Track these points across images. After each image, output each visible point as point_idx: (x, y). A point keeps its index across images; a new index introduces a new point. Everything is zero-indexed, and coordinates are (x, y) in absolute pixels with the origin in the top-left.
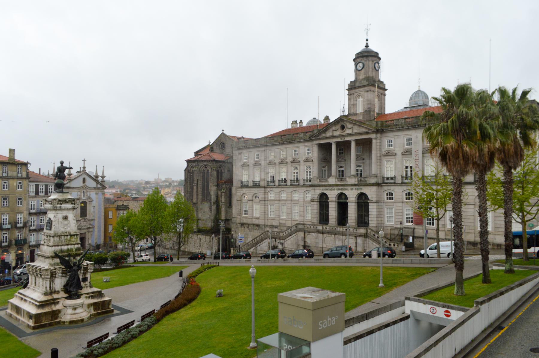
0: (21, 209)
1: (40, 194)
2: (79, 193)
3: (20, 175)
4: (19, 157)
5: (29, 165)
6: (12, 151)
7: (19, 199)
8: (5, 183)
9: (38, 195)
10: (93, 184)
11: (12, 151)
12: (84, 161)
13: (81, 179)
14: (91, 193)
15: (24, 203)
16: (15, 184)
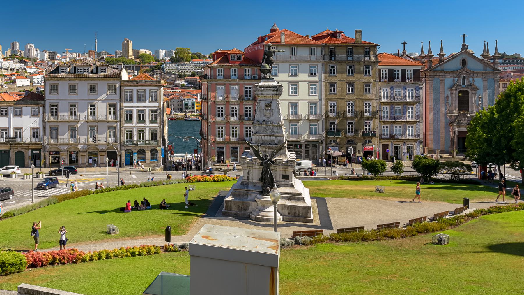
0: (369, 97)
1: (396, 80)
2: (456, 79)
3: (366, 59)
4: (367, 38)
5: (378, 47)
6: (358, 32)
7: (366, 85)
8: (350, 67)
9: (393, 81)
10: (480, 67)
11: (358, 32)
12: (464, 36)
13: (459, 61)
14: (476, 79)
15: (373, 89)
16: (362, 69)
